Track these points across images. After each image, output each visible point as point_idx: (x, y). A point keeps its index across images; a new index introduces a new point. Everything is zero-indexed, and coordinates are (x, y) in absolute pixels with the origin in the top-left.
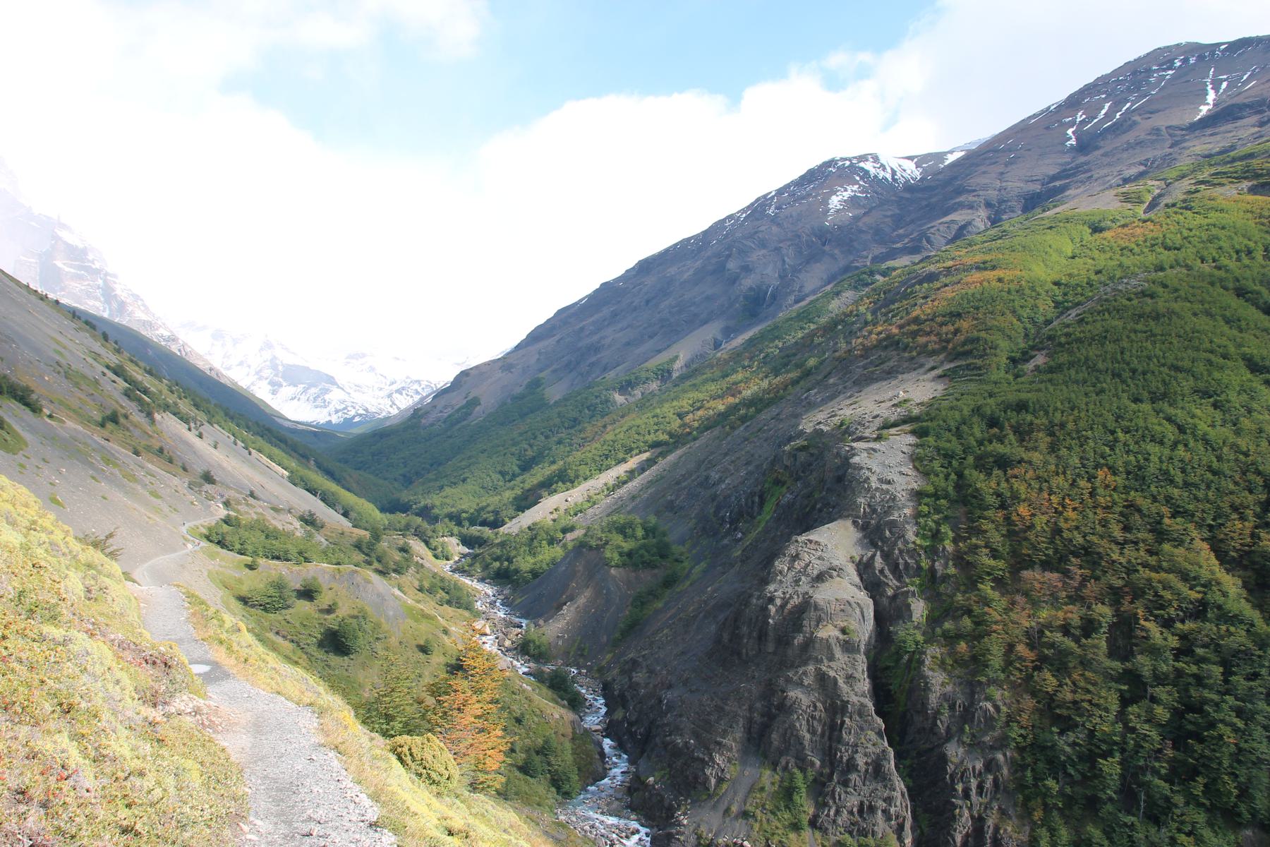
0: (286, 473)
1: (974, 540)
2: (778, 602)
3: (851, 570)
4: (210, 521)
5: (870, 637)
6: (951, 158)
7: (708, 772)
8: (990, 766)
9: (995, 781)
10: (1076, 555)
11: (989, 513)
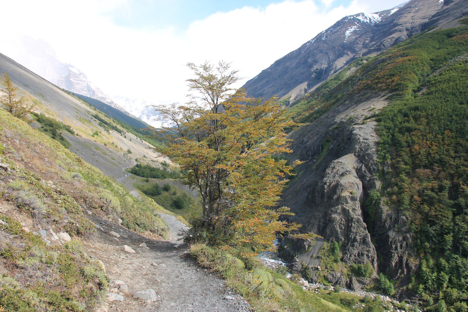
1: (398, 159)
2: (328, 184)
3: (354, 172)
4: (132, 166)
5: (361, 195)
6: (393, 12)
7: (305, 243)
8: (405, 239)
9: (407, 244)
10: (436, 163)
11: (403, 149)
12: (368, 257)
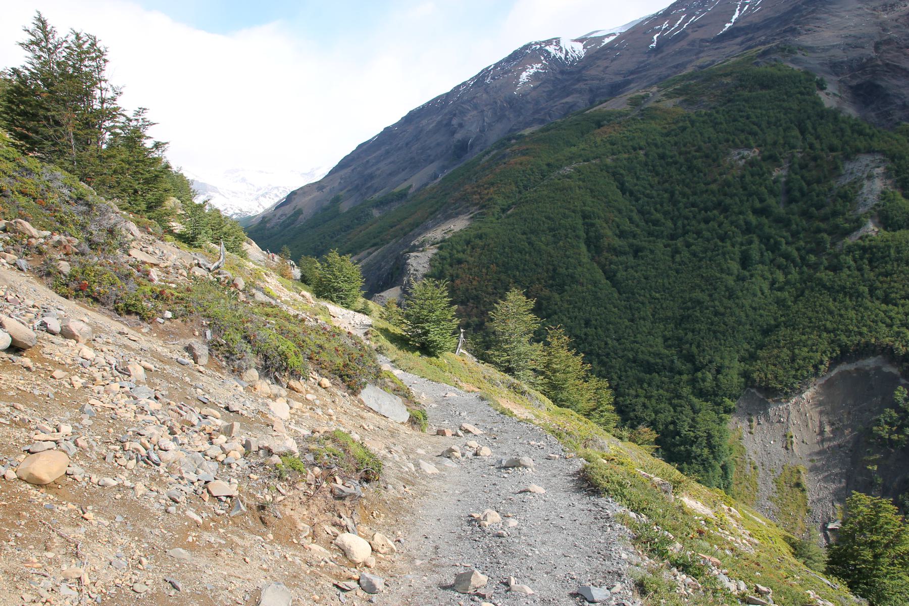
6: (607, 41)
10: (473, 299)
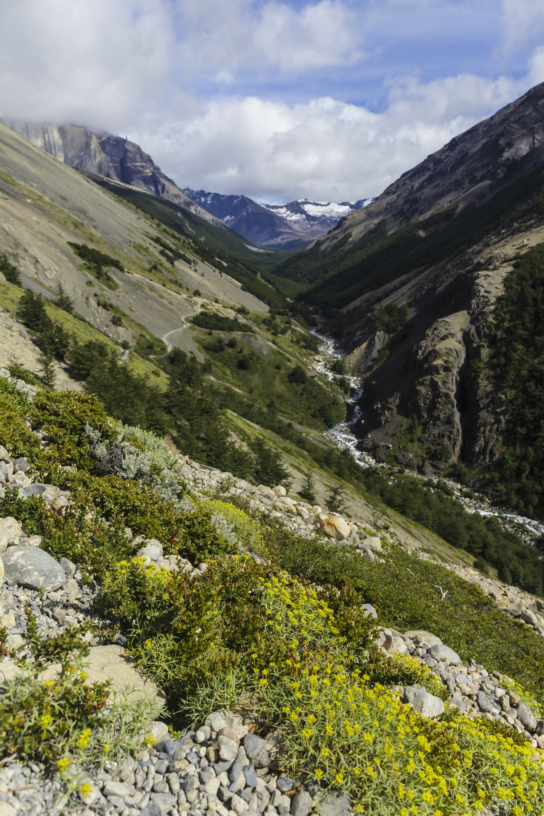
0: (240, 284)
3: (460, 335)
4: (193, 314)
9: (498, 427)
12: (449, 439)
